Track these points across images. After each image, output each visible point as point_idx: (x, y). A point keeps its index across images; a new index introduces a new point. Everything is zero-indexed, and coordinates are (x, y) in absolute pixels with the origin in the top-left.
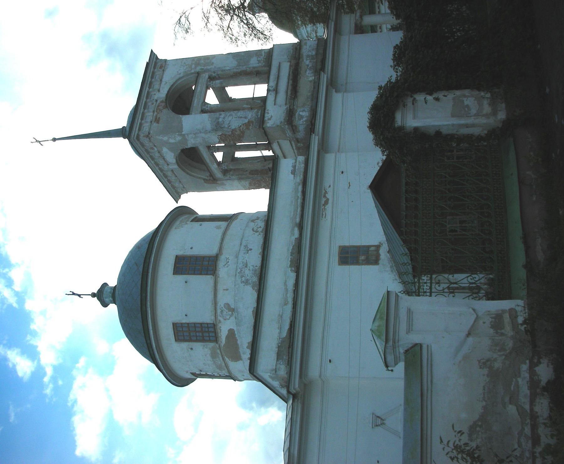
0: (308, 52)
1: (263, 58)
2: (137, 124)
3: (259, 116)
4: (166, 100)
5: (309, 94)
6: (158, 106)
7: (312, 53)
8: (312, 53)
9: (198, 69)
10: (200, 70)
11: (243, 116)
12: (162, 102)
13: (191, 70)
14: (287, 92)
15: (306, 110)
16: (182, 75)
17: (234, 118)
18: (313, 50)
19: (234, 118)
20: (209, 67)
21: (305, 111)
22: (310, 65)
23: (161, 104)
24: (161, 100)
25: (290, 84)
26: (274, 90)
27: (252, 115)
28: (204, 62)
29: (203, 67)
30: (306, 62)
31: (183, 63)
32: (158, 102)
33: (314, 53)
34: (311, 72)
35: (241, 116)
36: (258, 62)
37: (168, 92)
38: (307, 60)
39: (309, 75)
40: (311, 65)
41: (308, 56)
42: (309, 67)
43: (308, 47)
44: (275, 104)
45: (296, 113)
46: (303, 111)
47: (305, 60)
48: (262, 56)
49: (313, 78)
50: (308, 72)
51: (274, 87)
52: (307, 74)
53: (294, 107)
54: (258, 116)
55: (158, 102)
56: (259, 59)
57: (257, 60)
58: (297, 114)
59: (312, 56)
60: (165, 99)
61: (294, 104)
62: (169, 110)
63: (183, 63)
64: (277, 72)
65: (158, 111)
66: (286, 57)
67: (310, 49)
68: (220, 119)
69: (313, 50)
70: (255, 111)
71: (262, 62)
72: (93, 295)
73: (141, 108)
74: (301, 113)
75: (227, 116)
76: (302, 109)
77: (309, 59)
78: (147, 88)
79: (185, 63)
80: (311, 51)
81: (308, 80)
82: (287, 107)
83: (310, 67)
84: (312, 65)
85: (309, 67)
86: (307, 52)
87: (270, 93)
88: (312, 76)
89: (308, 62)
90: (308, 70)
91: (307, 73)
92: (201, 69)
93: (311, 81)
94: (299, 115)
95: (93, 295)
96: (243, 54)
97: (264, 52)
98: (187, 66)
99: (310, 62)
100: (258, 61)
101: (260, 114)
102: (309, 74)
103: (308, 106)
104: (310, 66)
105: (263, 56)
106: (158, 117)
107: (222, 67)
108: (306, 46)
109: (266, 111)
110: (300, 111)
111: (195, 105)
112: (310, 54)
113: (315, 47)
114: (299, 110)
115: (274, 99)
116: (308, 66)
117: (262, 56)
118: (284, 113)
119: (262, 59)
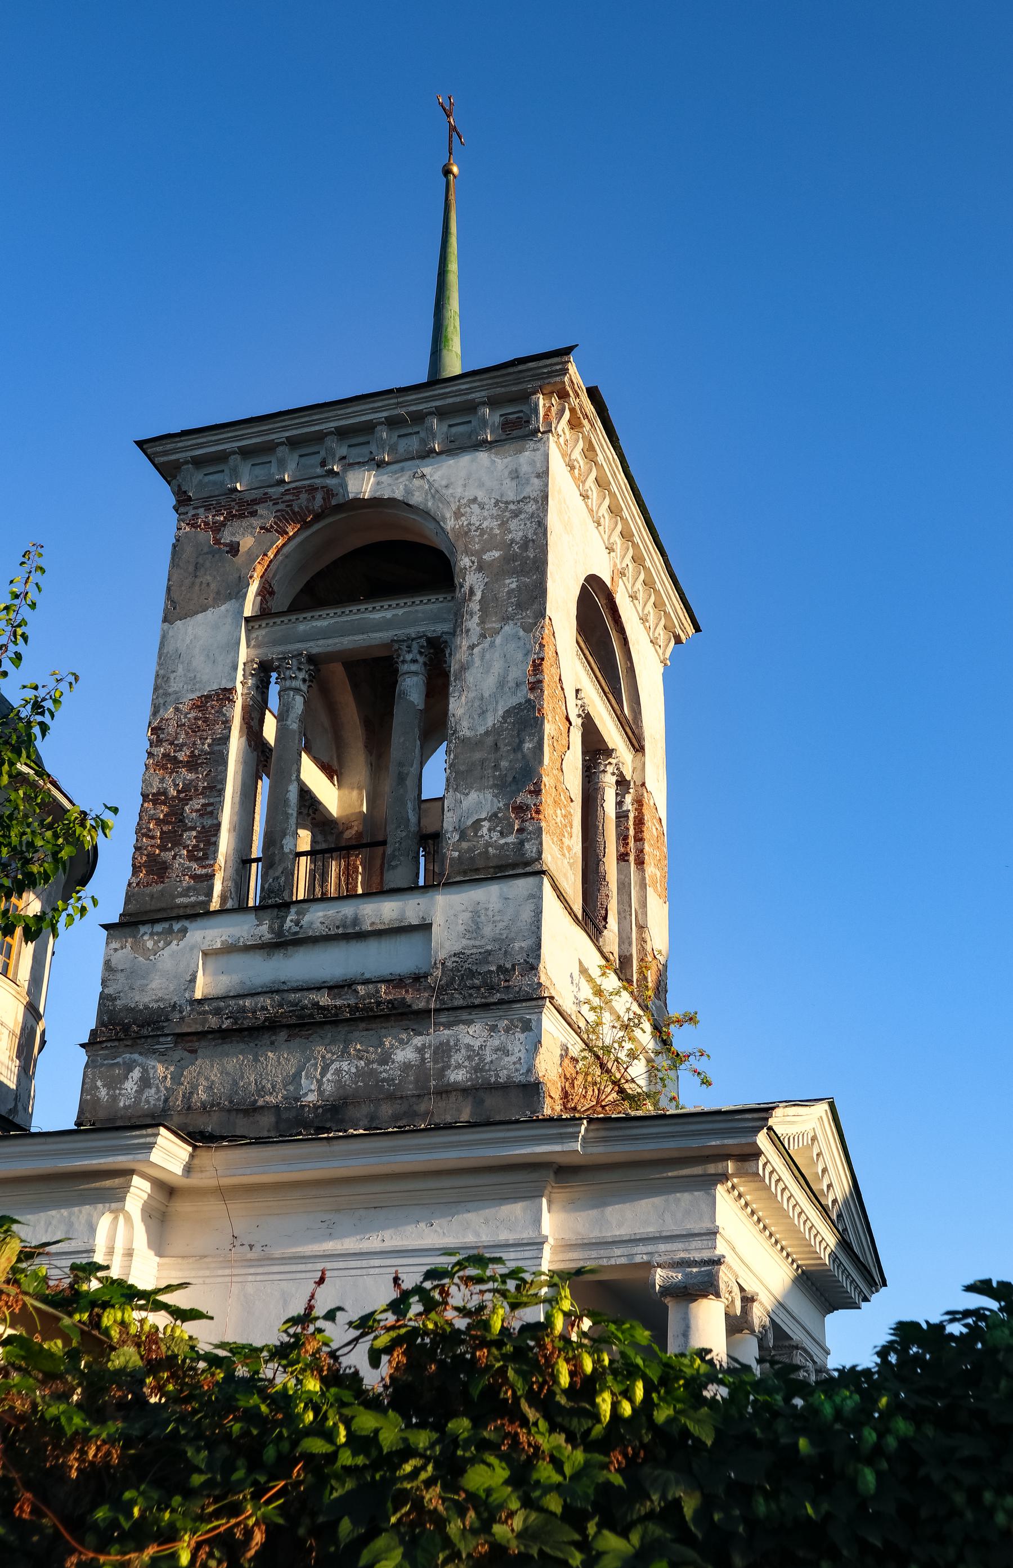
0: (469, 1047)
1: (488, 845)
2: (217, 442)
3: (179, 901)
4: (340, 508)
6: (312, 490)
8: (459, 1066)
9: (473, 581)
12: (329, 493)
20: (473, 624)
21: (140, 1092)
22: (385, 1072)
23: (319, 496)
26: (280, 933)
29: (478, 596)
32: (331, 482)
33: (458, 1076)
38: (421, 1050)
40: (384, 1075)
41: (443, 1051)
46: (145, 1082)
47: (418, 1041)
49: (312, 1097)
54: (181, 895)
56: (486, 824)
57: (478, 822)
58: (136, 1056)
59: (441, 1073)
60: (342, 501)
65: (287, 498)
66: (457, 948)
73: (285, 428)
74: (136, 1074)
77: (423, 1059)
78: (385, 414)
79: (516, 514)
80: (469, 1058)
84: (384, 1080)
85: (375, 1066)
88: (321, 1093)
89: (406, 1055)
91: (345, 1065)
94: (130, 1069)
96: (528, 745)
99: (407, 1066)
100: (477, 824)
101: (193, 899)
102: (338, 1072)
109: (176, 927)
111: (302, 627)
112: (458, 1058)
113: (497, 1076)
116: (385, 1059)
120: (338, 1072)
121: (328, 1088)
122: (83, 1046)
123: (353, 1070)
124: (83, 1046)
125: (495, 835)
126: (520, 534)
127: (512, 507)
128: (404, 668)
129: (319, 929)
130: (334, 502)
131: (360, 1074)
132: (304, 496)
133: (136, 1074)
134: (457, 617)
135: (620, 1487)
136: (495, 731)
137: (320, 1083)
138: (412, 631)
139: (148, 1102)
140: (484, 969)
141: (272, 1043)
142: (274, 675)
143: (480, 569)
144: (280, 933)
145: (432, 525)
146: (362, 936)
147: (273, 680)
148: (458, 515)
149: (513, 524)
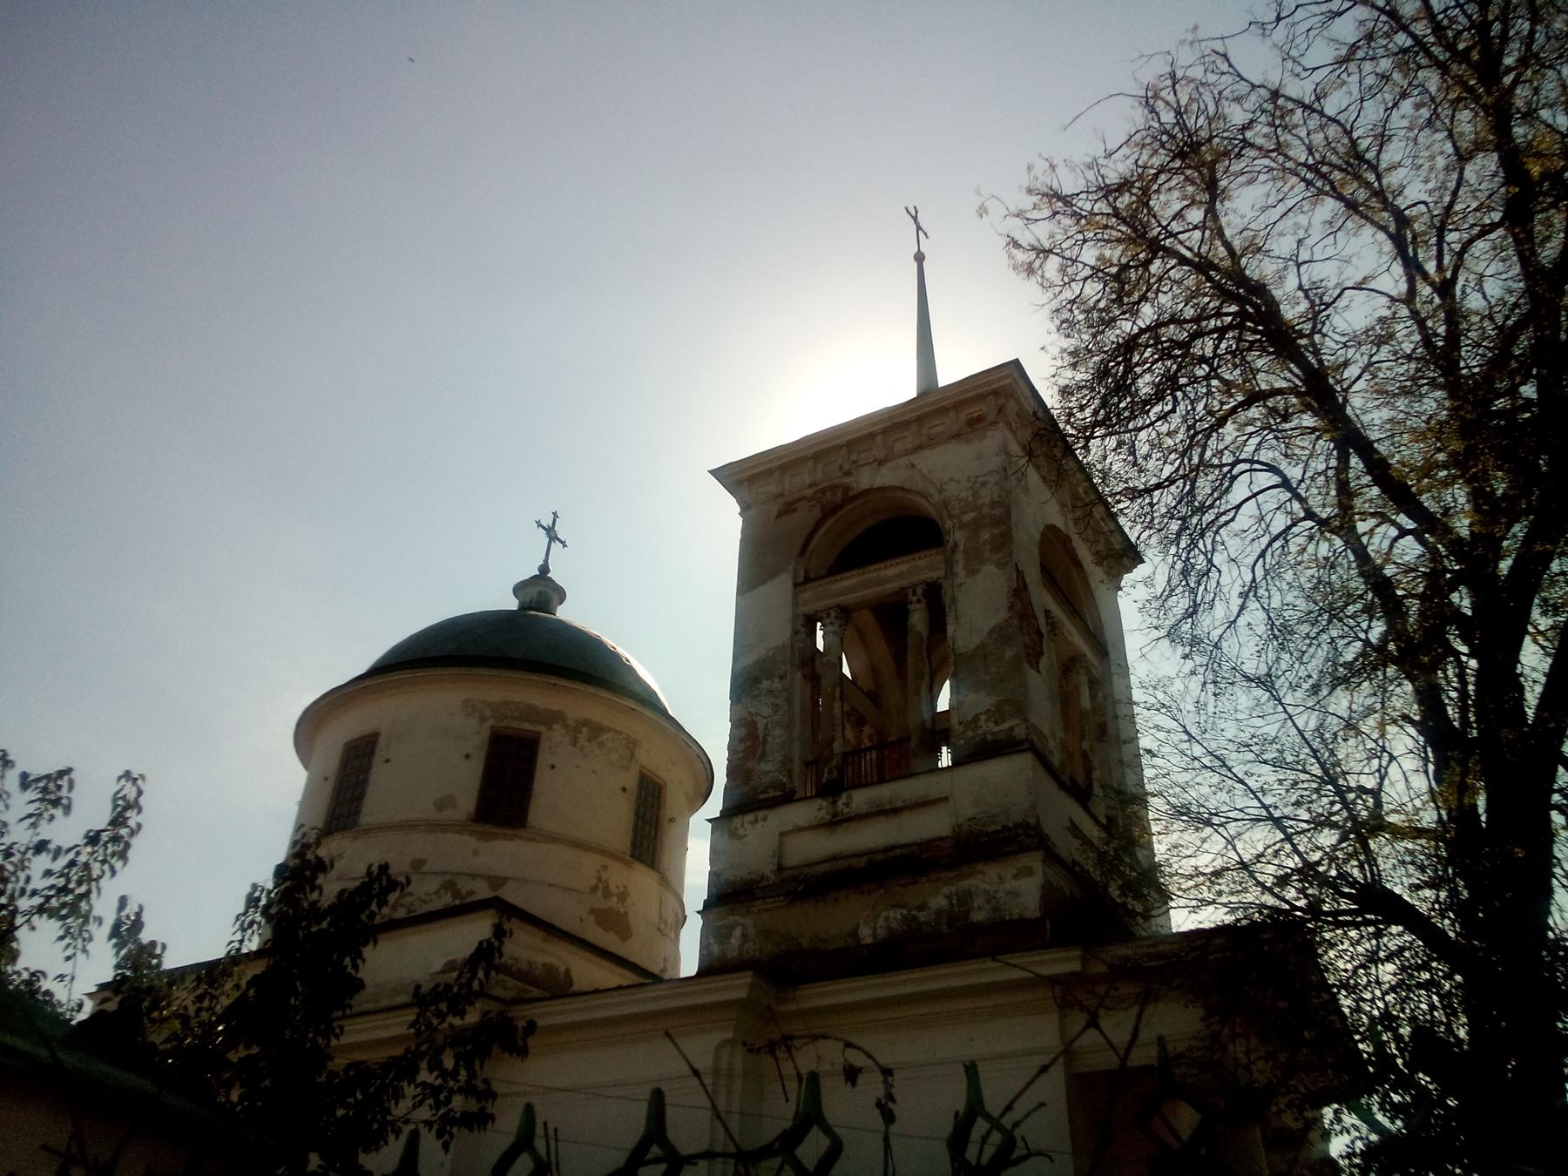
0: (986, 892)
3: (762, 796)
4: (855, 498)
5: (805, 943)
6: (834, 488)
7: (980, 908)
9: (958, 537)
10: (951, 544)
11: (767, 747)
12: (846, 489)
13: (951, 517)
14: (835, 858)
15: (749, 945)
16: (937, 498)
17: (765, 721)
18: (996, 909)
19: (765, 721)
24: (855, 485)
25: (854, 862)
27: (766, 773)
28: (986, 540)
29: (962, 547)
30: (937, 898)
31: (987, 478)
33: (978, 916)
34: (895, 926)
35: (769, 738)
36: (969, 718)
37: (883, 489)
38: (948, 897)
39: (881, 922)
40: (923, 919)
41: (966, 897)
42: (915, 912)
43: (1010, 885)
44: (782, 834)
45: (740, 915)
46: (744, 937)
47: (946, 890)
48: (996, 723)
49: (869, 941)
50: (896, 915)
51: (846, 810)
52: (884, 914)
53: (760, 901)
55: (847, 480)
56: (983, 718)
57: (977, 715)
58: (737, 918)
59: (968, 912)
60: (856, 493)
61: (768, 900)
62: (819, 524)
63: (987, 478)
64: (904, 801)
65: (819, 495)
66: (970, 814)
67: (1000, 895)
68: (769, 682)
69: (996, 909)
70: (781, 777)
71: (970, 733)
72: (544, 569)
74: (738, 932)
75: (773, 700)
76: (751, 930)
77: (952, 905)
79: (984, 484)
80: (988, 902)
81: (862, 923)
82: (768, 879)
83: (915, 918)
85: (915, 912)
86: (986, 886)
87: (825, 804)
88: (874, 935)
89: (938, 902)
90: (905, 912)
91: (892, 914)
92: (956, 545)
93: (854, 934)
95: (544, 569)
97: (1011, 729)
98: (970, 499)
99: (940, 912)
100: (976, 718)
101: (771, 795)
102: (887, 919)
103: (761, 951)
104: (920, 914)
105: (996, 729)
106: (797, 505)
107: (956, 610)
108: (1015, 877)
109: (761, 814)
110: (743, 926)
112: (978, 902)
113: (1010, 915)
114: (749, 921)
115: (802, 823)
117: (996, 723)
118: (750, 874)
119: (980, 732)
120: (887, 919)
121: (881, 933)
122: (698, 912)
123: (899, 917)
124: (698, 912)
125: (991, 725)
126: (989, 497)
127: (980, 479)
128: (912, 607)
129: (864, 809)
130: (851, 494)
131: (905, 919)
132: (828, 493)
133: (738, 932)
134: (949, 564)
135: (269, 968)
136: (982, 646)
137: (875, 929)
138: (915, 579)
139: (748, 953)
140: (992, 828)
141: (836, 899)
142: (819, 624)
143: (960, 528)
144: (834, 816)
145: (922, 502)
146: (895, 811)
147: (818, 628)
148: (940, 491)
149: (983, 492)
